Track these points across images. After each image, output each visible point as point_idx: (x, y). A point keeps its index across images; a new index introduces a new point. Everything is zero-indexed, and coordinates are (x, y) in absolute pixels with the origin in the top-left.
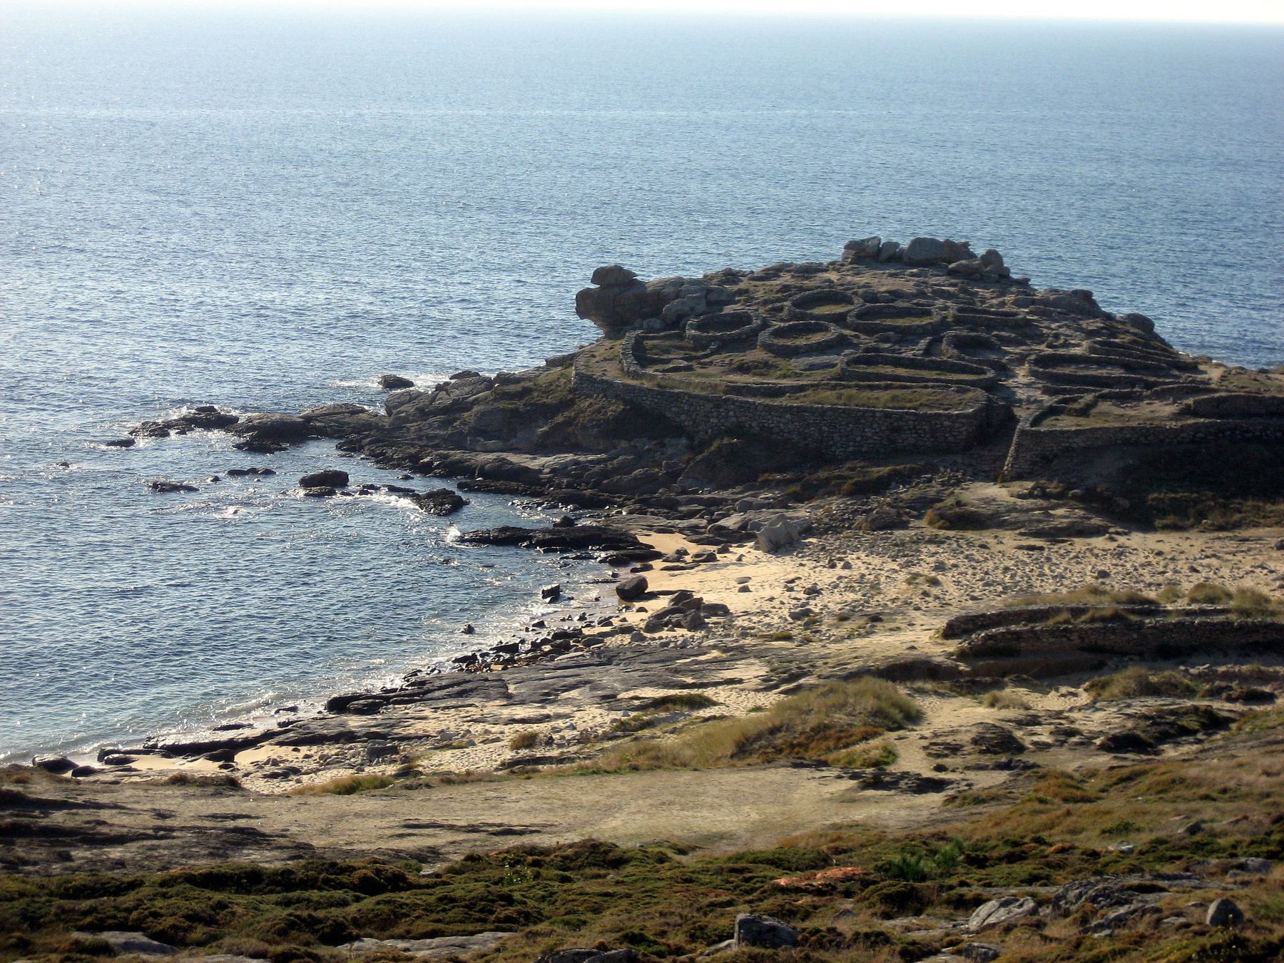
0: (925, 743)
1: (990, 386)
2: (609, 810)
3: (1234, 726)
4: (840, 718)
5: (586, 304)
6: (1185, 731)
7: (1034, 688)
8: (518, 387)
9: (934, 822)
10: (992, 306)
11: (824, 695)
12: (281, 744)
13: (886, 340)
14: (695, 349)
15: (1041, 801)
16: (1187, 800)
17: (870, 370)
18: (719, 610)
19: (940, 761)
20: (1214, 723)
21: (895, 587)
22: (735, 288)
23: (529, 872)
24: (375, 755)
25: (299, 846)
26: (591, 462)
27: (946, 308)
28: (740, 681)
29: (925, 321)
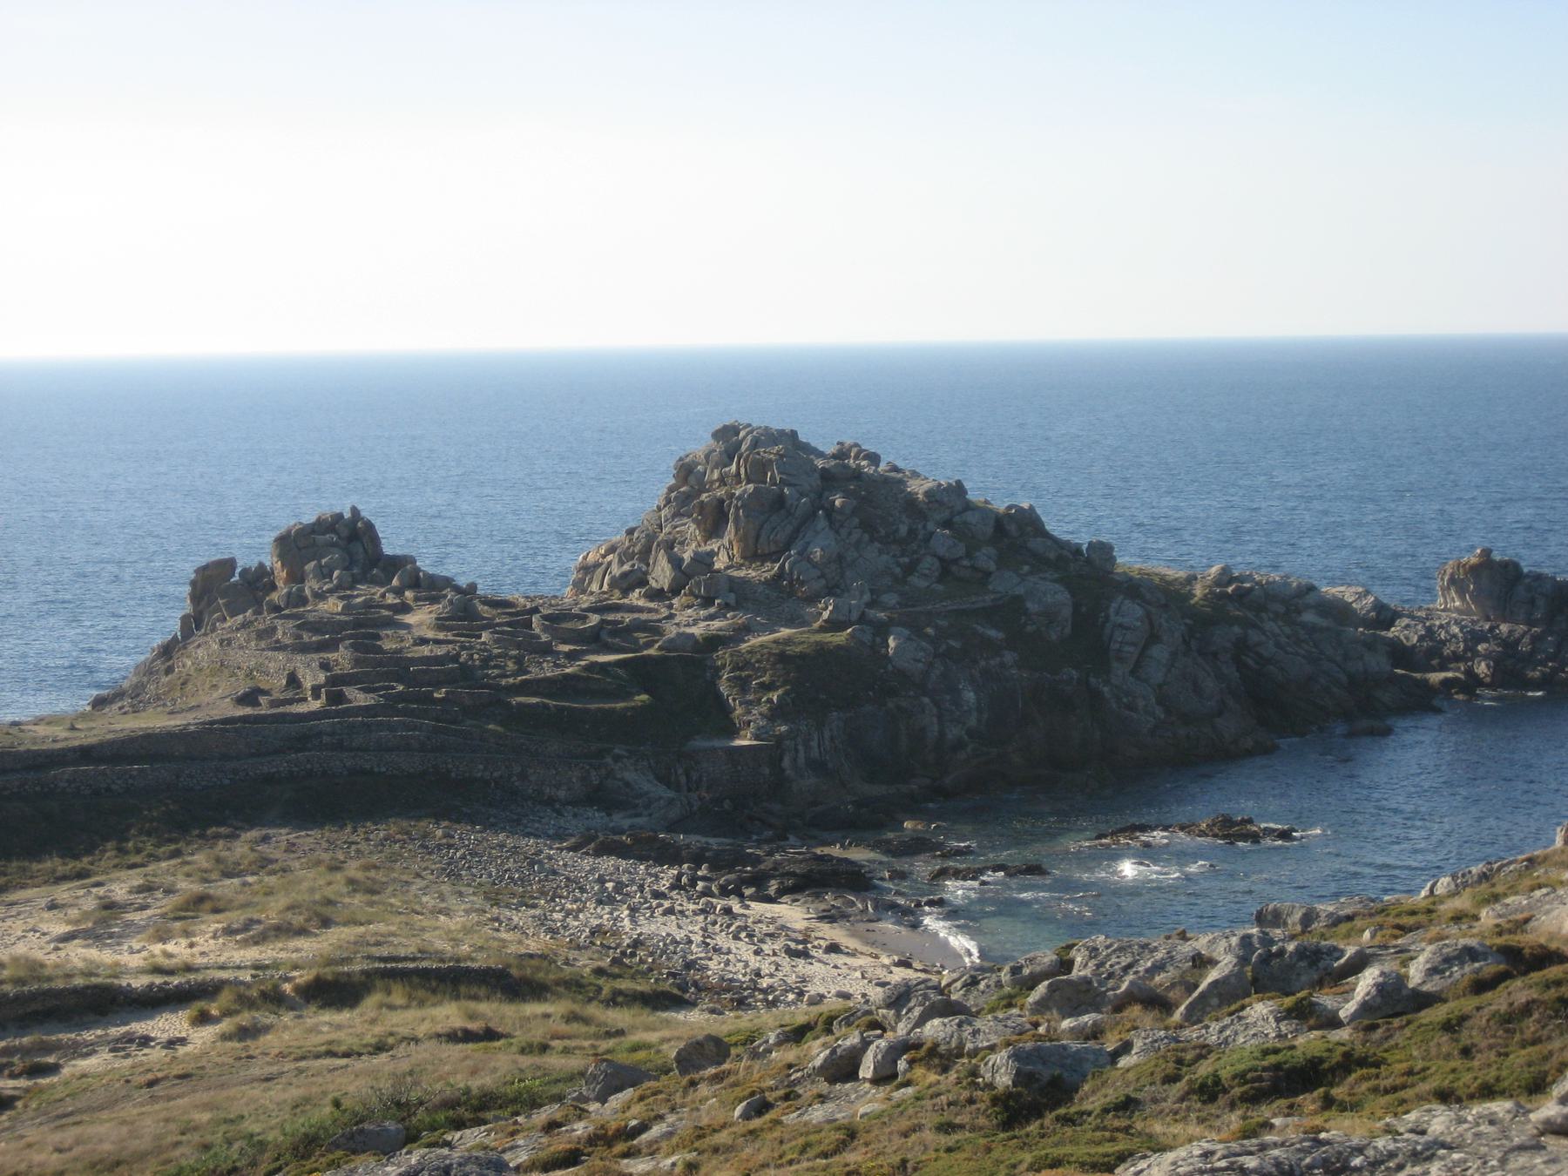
3: (19, 1104)
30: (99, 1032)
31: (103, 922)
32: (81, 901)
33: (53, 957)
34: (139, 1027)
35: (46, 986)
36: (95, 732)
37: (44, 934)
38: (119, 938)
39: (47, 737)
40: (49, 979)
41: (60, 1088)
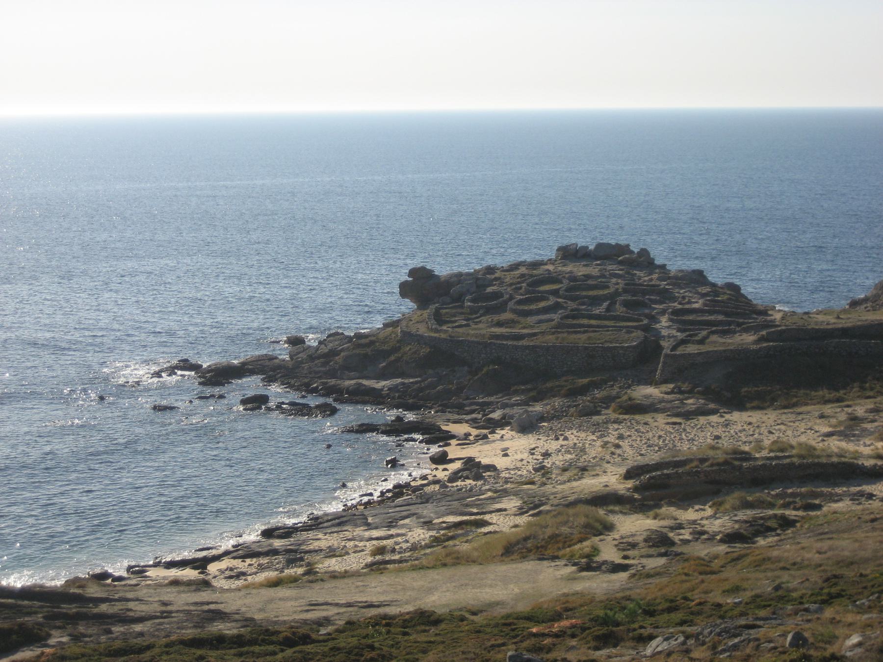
0: (616, 542)
1: (646, 329)
2: (430, 591)
3: (798, 525)
4: (565, 530)
5: (405, 290)
6: (770, 529)
7: (679, 507)
8: (367, 341)
9: (623, 590)
10: (645, 281)
11: (555, 516)
12: (234, 558)
13: (583, 304)
14: (471, 314)
15: (686, 575)
16: (773, 570)
17: (575, 322)
18: (491, 468)
19: (625, 553)
20: (786, 523)
21: (595, 450)
22: (493, 277)
23: (384, 630)
24: (290, 563)
25: (247, 620)
26: (412, 383)
27: (617, 284)
28: (505, 510)
29: (606, 292)
30: (845, 489)
31: (850, 428)
32: (838, 415)
33: (821, 445)
34: (868, 488)
35: (816, 460)
36: (851, 320)
37: (816, 432)
38: (858, 437)
39: (823, 322)
40: (818, 457)
41: (821, 518)
